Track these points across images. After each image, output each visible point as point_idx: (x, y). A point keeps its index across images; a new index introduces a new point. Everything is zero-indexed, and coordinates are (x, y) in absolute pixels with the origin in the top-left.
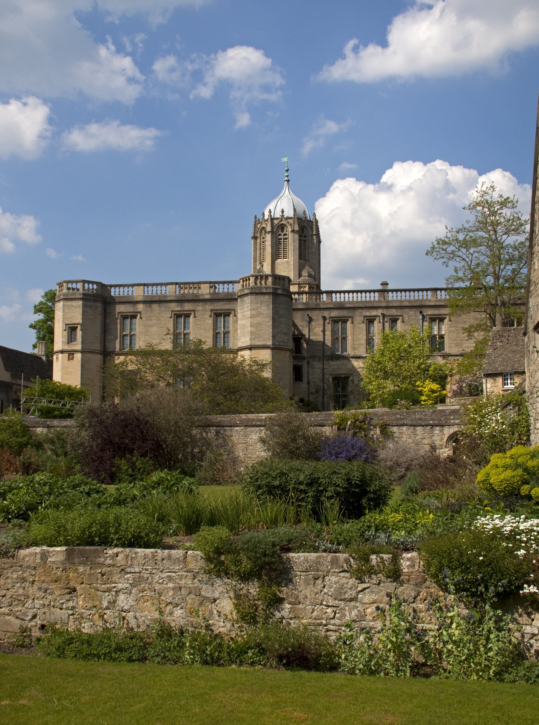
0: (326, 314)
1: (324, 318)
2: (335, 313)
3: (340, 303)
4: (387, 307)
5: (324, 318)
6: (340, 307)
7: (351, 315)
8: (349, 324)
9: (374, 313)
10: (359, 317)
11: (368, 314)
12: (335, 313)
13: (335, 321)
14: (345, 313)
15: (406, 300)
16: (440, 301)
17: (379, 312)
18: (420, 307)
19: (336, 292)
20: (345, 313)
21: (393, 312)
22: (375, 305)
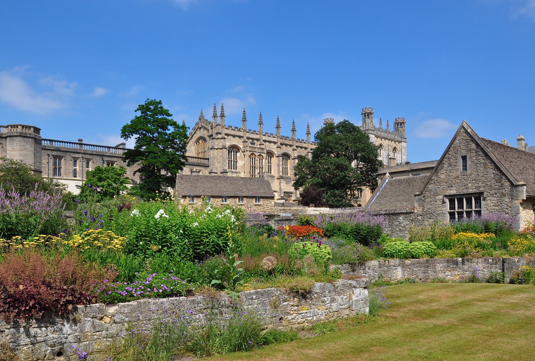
0: (50, 152)
1: (48, 155)
2: (55, 153)
3: (57, 148)
4: (84, 154)
5: (48, 155)
6: (58, 150)
7: (64, 155)
8: (63, 160)
9: (77, 156)
10: (69, 156)
11: (74, 156)
12: (55, 153)
13: (55, 157)
14: (61, 154)
15: (94, 151)
16: (112, 153)
17: (80, 156)
18: (102, 156)
19: (55, 141)
20: (61, 154)
21: (88, 156)
22: (78, 151)
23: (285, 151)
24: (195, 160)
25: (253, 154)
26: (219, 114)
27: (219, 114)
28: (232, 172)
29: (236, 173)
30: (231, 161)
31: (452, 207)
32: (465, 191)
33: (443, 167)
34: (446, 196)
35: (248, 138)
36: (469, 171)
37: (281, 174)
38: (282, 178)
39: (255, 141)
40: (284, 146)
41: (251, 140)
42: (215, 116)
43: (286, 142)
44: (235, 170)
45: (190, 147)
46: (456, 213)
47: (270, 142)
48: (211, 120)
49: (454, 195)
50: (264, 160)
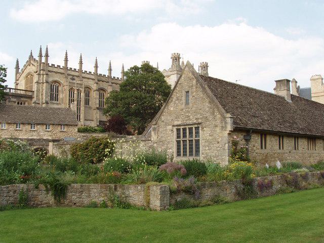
23: (101, 86)
24: (23, 92)
25: (72, 88)
26: (44, 54)
27: (44, 54)
28: (54, 103)
29: (57, 104)
30: (53, 94)
31: (178, 137)
32: (188, 122)
33: (172, 100)
34: (174, 126)
35: (70, 75)
36: (191, 105)
37: (98, 106)
38: (98, 108)
39: (75, 78)
40: (101, 82)
41: (71, 77)
42: (41, 56)
43: (103, 79)
44: (56, 102)
45: (21, 81)
46: (181, 141)
47: (89, 79)
48: (37, 59)
49: (180, 125)
50: (82, 94)
